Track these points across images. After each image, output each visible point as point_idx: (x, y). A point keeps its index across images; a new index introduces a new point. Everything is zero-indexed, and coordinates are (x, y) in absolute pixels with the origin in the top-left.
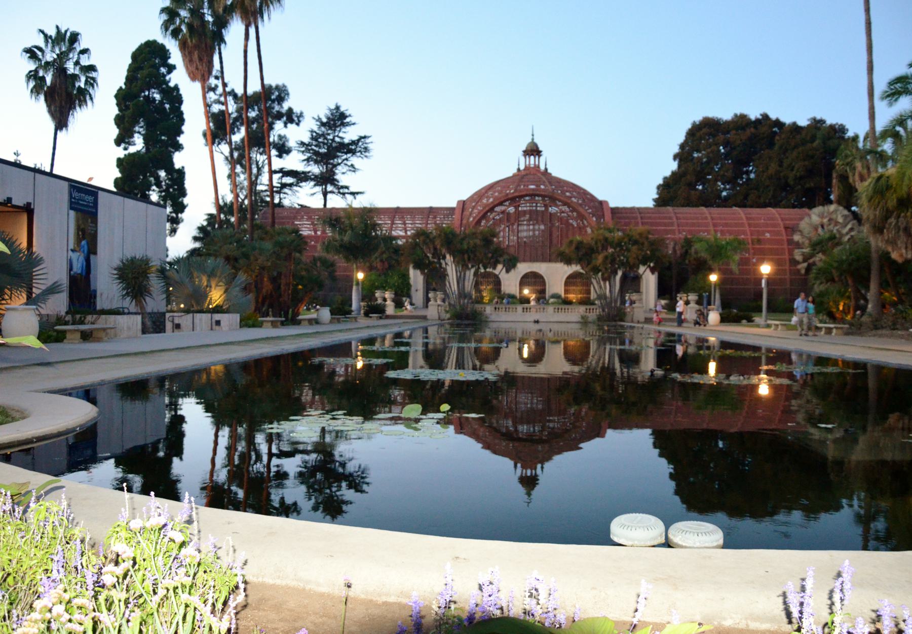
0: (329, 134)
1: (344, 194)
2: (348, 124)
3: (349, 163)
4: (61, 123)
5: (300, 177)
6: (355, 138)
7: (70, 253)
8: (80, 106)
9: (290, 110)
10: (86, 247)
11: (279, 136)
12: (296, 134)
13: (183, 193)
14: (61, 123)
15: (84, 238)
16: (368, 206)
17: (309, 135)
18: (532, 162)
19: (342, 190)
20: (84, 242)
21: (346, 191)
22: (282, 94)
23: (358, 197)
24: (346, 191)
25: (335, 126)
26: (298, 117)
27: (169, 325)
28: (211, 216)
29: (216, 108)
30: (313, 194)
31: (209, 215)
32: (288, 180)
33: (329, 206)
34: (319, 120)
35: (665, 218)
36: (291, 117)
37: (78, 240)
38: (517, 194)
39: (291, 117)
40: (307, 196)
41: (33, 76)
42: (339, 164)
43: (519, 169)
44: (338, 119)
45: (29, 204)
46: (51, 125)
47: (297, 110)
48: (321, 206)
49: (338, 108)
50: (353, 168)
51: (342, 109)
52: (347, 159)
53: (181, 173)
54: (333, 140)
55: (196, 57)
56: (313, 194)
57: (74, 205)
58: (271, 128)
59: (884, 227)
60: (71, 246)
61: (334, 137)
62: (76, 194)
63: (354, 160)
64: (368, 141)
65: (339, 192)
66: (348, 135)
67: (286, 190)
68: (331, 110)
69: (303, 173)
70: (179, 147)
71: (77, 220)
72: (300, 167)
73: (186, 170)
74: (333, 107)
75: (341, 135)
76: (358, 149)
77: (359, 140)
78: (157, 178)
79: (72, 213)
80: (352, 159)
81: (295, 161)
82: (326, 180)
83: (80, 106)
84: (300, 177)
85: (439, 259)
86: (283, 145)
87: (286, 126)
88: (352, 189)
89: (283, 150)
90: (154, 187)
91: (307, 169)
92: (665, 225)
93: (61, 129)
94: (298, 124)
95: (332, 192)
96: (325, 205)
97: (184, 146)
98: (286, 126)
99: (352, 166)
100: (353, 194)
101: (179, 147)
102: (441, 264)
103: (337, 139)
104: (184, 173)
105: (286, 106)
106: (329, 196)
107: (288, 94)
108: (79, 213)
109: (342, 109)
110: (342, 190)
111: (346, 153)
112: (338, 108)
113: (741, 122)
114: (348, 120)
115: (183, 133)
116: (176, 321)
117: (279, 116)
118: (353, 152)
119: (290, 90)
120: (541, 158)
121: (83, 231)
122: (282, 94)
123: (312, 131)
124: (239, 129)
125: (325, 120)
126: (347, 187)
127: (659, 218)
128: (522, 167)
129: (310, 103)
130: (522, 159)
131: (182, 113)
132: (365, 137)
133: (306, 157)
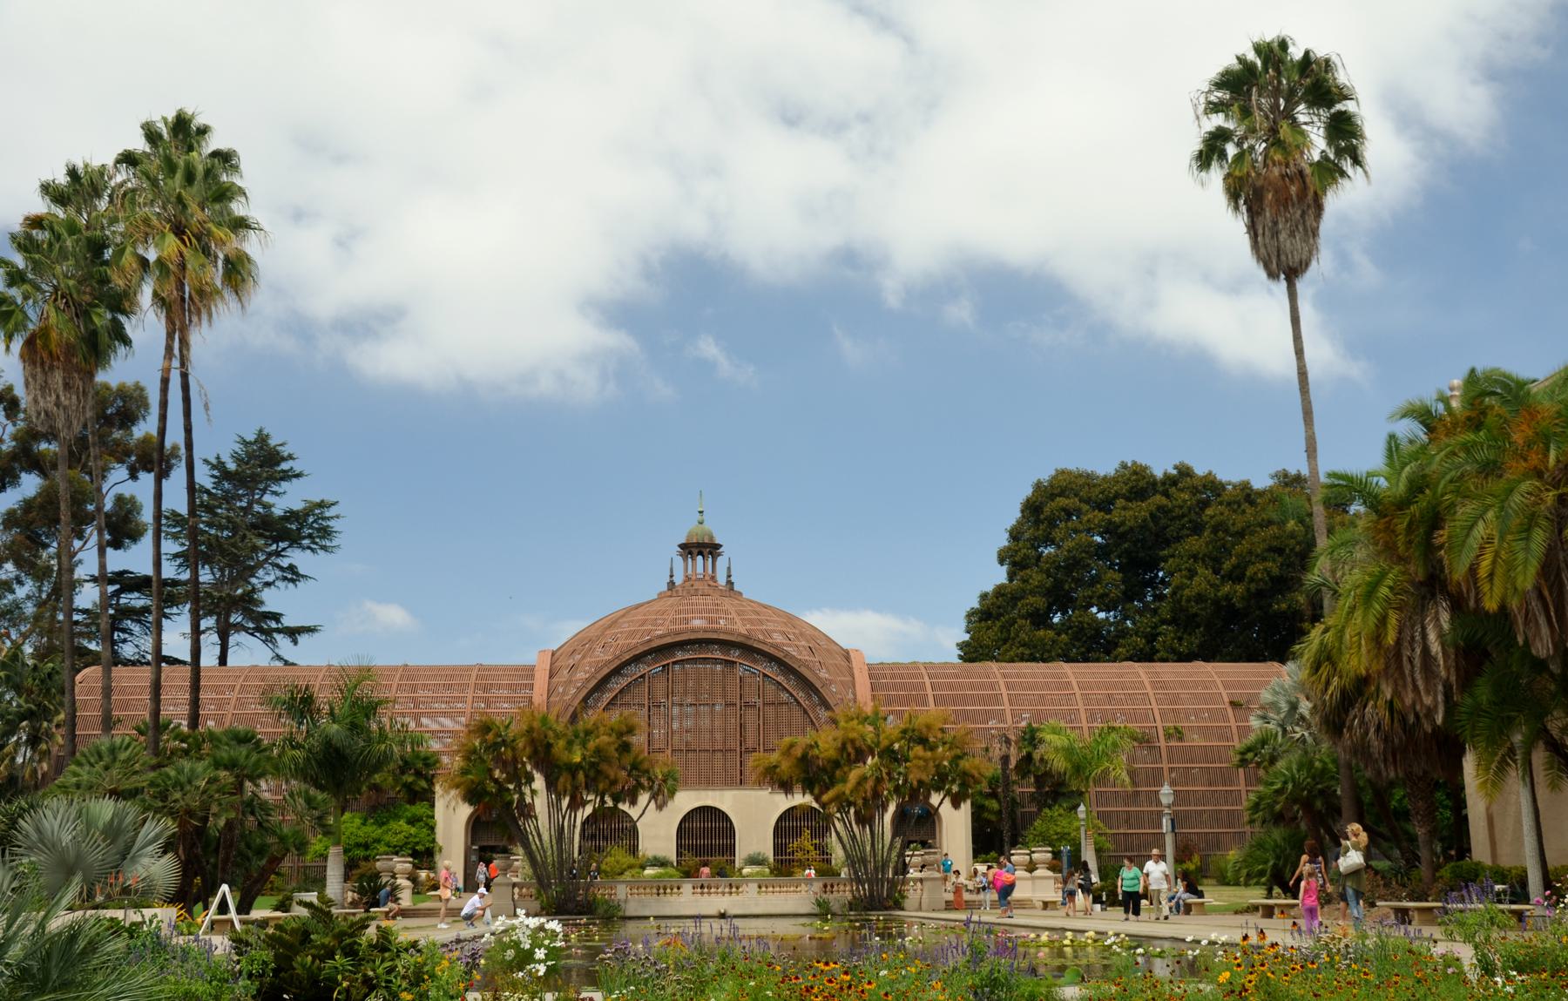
0: (240, 498)
1: (268, 633)
2: (287, 476)
3: (285, 563)
5: (166, 595)
6: (298, 506)
11: (120, 499)
16: (353, 663)
18: (700, 569)
19: (266, 625)
21: (274, 625)
24: (274, 625)
25: (255, 479)
32: (135, 600)
35: (982, 686)
42: (260, 565)
43: (672, 584)
44: (263, 463)
49: (262, 439)
50: (293, 575)
52: (278, 554)
55: (58, 378)
59: (1343, 725)
61: (250, 504)
63: (297, 557)
65: (259, 629)
66: (285, 499)
67: (128, 623)
68: (245, 443)
74: (251, 437)
75: (267, 498)
76: (307, 531)
77: (307, 512)
80: (289, 552)
84: (166, 595)
85: (519, 786)
88: (287, 622)
92: (983, 700)
95: (239, 628)
96: (223, 660)
98: (133, 476)
99: (292, 568)
100: (293, 633)
102: (522, 794)
103: (257, 508)
106: (234, 638)
109: (272, 442)
110: (266, 625)
111: (276, 540)
112: (262, 439)
113: (1137, 484)
114: (284, 466)
118: (295, 540)
125: (232, 466)
126: (276, 617)
127: (972, 686)
128: (678, 580)
130: (679, 561)
132: (322, 505)
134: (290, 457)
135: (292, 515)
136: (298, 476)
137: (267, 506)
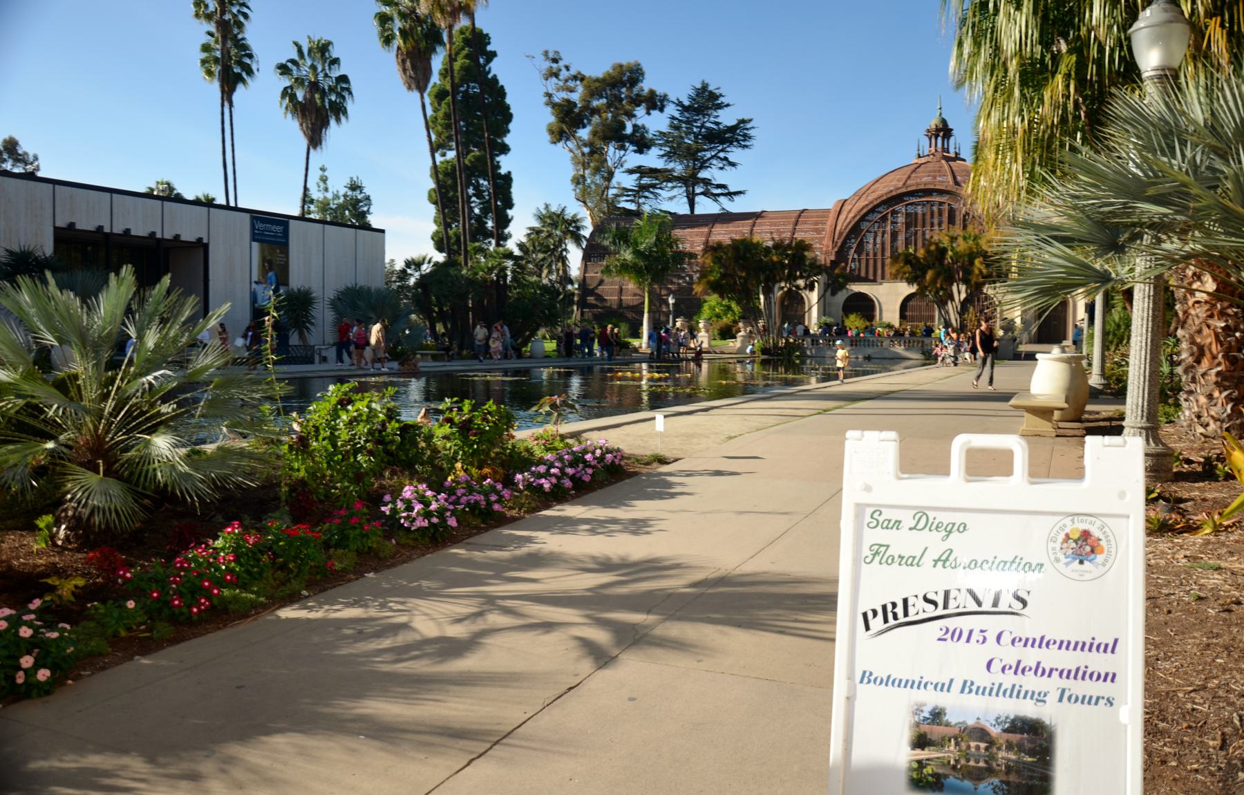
0: (696, 121)
2: (720, 106)
4: (315, 140)
6: (731, 122)
7: (254, 285)
8: (338, 120)
9: (652, 92)
10: (274, 278)
12: (656, 123)
13: (510, 205)
14: (315, 140)
15: (271, 269)
17: (668, 121)
20: (270, 274)
22: (632, 75)
23: (736, 198)
26: (662, 101)
27: (317, 358)
28: (536, 231)
29: (559, 97)
30: (671, 199)
31: (530, 229)
33: (697, 212)
34: (680, 104)
36: (654, 102)
37: (264, 272)
38: (904, 190)
39: (654, 102)
40: (672, 201)
41: (287, 93)
44: (706, 100)
45: (200, 240)
46: (304, 142)
47: (660, 91)
48: (688, 212)
49: (705, 87)
51: (710, 88)
52: (722, 150)
53: (508, 178)
54: (702, 126)
56: (671, 199)
57: (255, 237)
58: (631, 115)
60: (255, 278)
62: (259, 225)
63: (735, 154)
64: (749, 126)
66: (727, 118)
67: (647, 194)
69: (666, 170)
70: (505, 149)
71: (262, 251)
72: (659, 164)
73: (513, 176)
74: (699, 86)
75: (712, 119)
78: (477, 187)
79: (255, 245)
81: (653, 159)
82: (690, 181)
83: (338, 120)
86: (643, 137)
87: (648, 113)
88: (732, 190)
89: (642, 143)
90: (474, 199)
91: (671, 166)
93: (315, 148)
94: (661, 110)
97: (511, 146)
99: (726, 159)
101: (505, 149)
103: (708, 125)
104: (511, 179)
105: (646, 85)
106: (697, 199)
107: (642, 74)
108: (265, 245)
109: (710, 88)
112: (705, 87)
114: (721, 100)
115: (508, 131)
116: (324, 354)
117: (637, 101)
118: (730, 142)
119: (645, 69)
120: (952, 139)
121: (270, 262)
122: (632, 75)
123: (673, 118)
124: (589, 121)
125: (687, 103)
129: (673, 80)
131: (508, 108)
132: (743, 121)
133: (662, 153)
134: (721, 95)
135: (732, 129)
136: (728, 105)
137: (717, 124)
